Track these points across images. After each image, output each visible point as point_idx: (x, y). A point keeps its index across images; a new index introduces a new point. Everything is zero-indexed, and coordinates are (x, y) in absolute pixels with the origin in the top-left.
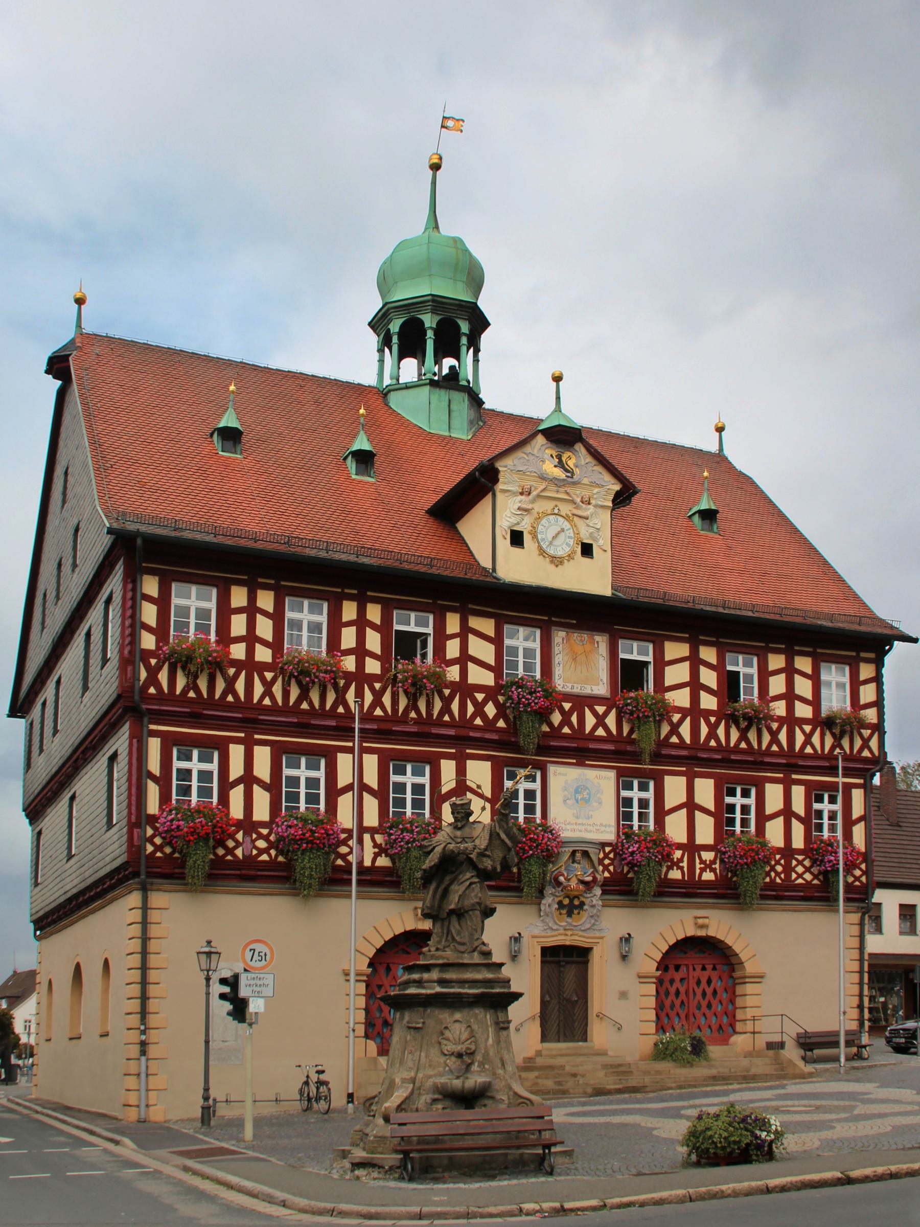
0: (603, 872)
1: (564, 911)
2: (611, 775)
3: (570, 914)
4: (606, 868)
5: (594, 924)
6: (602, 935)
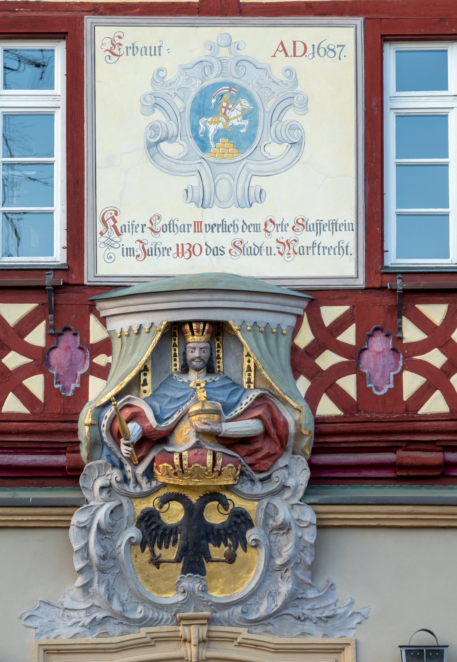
0: (312, 399)
1: (170, 553)
2: (345, 36)
3: (194, 561)
4: (324, 384)
5: (294, 599)
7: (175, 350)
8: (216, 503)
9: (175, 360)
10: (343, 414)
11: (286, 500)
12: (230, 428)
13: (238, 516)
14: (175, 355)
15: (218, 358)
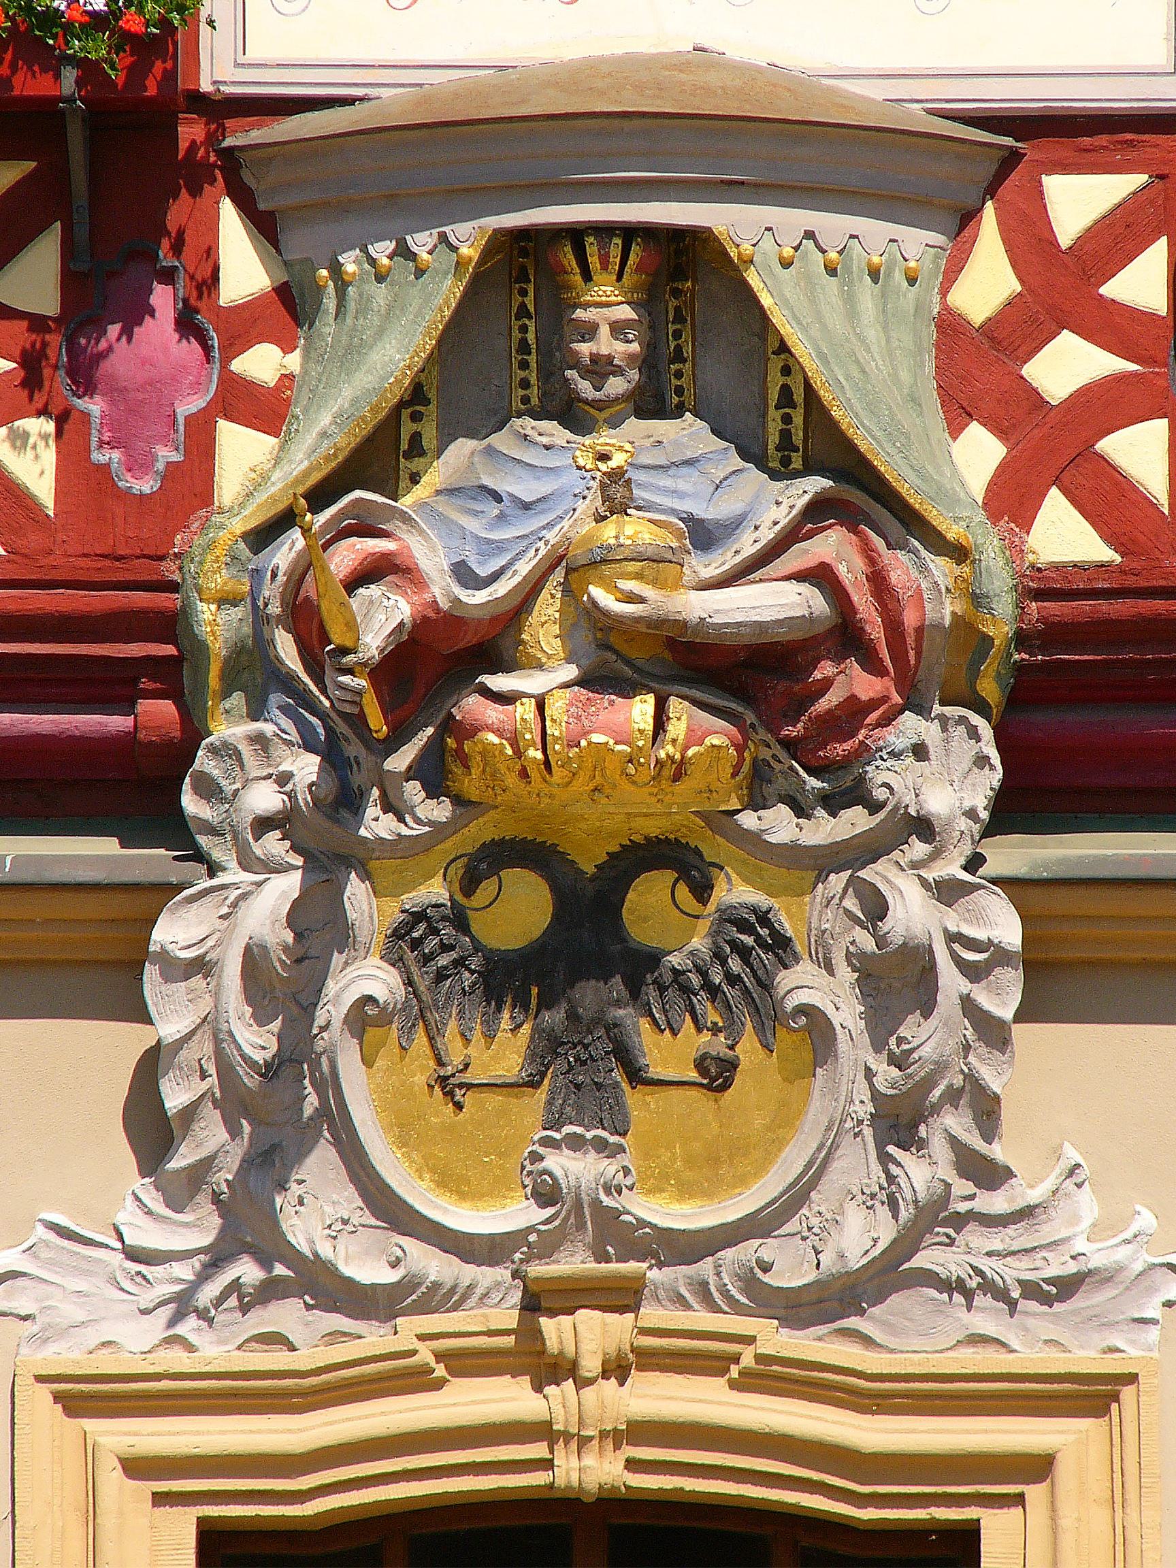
6: (1084, 1357)
7: (524, 329)
8: (669, 876)
9: (524, 365)
10: (1118, 559)
11: (914, 865)
12: (717, 611)
13: (744, 926)
14: (524, 347)
15: (678, 356)
